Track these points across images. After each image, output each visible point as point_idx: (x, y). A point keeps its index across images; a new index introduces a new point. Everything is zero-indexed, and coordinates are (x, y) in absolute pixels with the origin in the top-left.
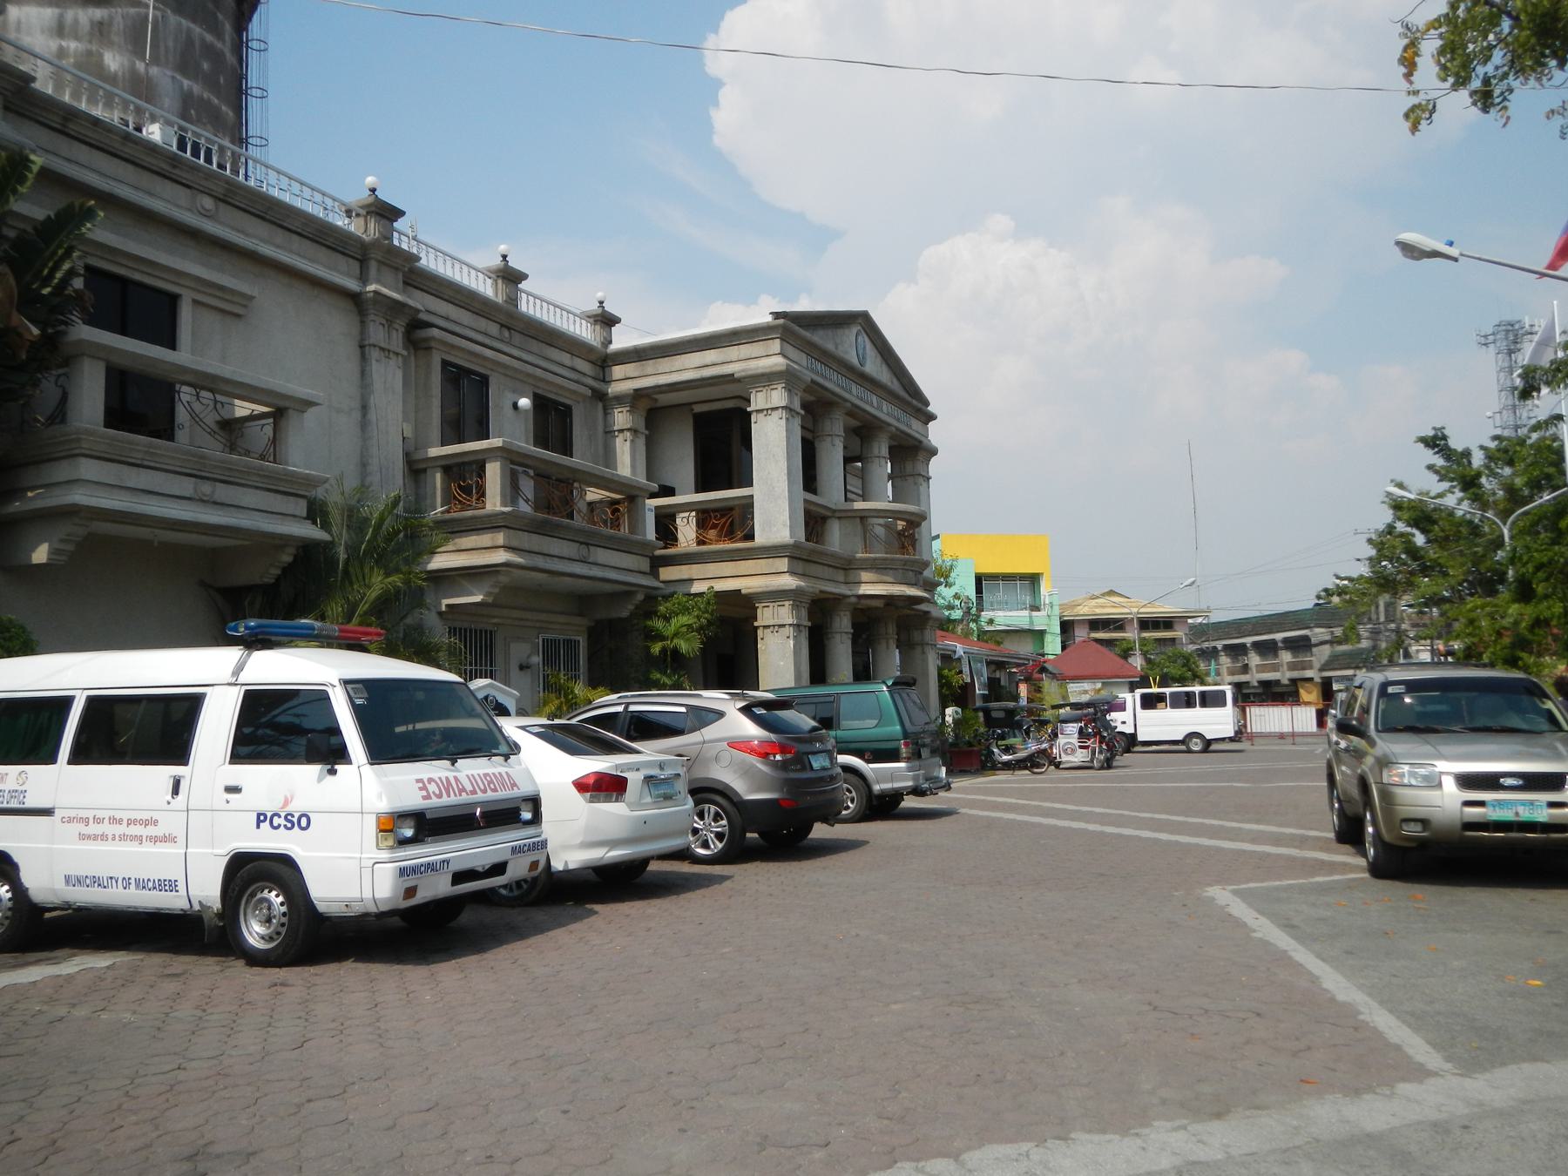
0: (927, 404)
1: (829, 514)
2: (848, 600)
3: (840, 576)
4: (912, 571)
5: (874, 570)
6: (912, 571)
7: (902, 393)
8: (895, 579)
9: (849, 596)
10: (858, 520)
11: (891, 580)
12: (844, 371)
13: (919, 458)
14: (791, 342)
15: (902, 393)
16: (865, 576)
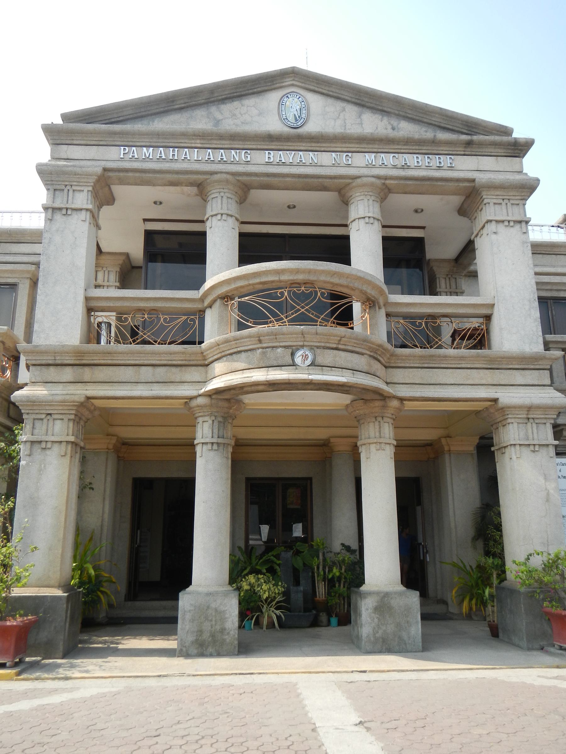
0: (506, 131)
1: (199, 306)
2: (194, 403)
3: (194, 374)
4: (281, 347)
5: (225, 359)
6: (281, 347)
7: (427, 133)
8: (249, 364)
9: (196, 397)
10: (218, 302)
11: (242, 365)
12: (226, 143)
13: (485, 201)
14: (75, 142)
15: (427, 133)
16: (218, 367)
